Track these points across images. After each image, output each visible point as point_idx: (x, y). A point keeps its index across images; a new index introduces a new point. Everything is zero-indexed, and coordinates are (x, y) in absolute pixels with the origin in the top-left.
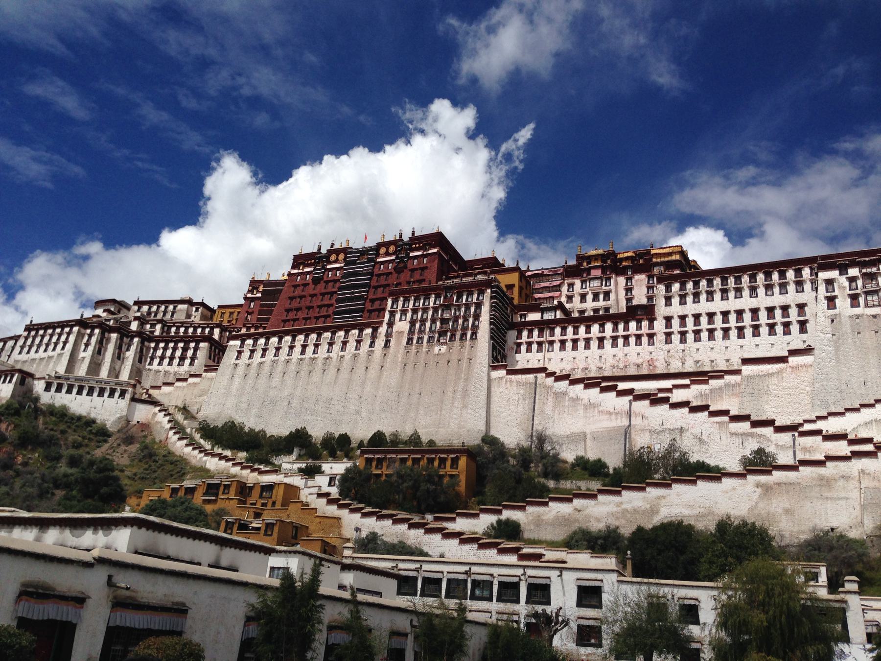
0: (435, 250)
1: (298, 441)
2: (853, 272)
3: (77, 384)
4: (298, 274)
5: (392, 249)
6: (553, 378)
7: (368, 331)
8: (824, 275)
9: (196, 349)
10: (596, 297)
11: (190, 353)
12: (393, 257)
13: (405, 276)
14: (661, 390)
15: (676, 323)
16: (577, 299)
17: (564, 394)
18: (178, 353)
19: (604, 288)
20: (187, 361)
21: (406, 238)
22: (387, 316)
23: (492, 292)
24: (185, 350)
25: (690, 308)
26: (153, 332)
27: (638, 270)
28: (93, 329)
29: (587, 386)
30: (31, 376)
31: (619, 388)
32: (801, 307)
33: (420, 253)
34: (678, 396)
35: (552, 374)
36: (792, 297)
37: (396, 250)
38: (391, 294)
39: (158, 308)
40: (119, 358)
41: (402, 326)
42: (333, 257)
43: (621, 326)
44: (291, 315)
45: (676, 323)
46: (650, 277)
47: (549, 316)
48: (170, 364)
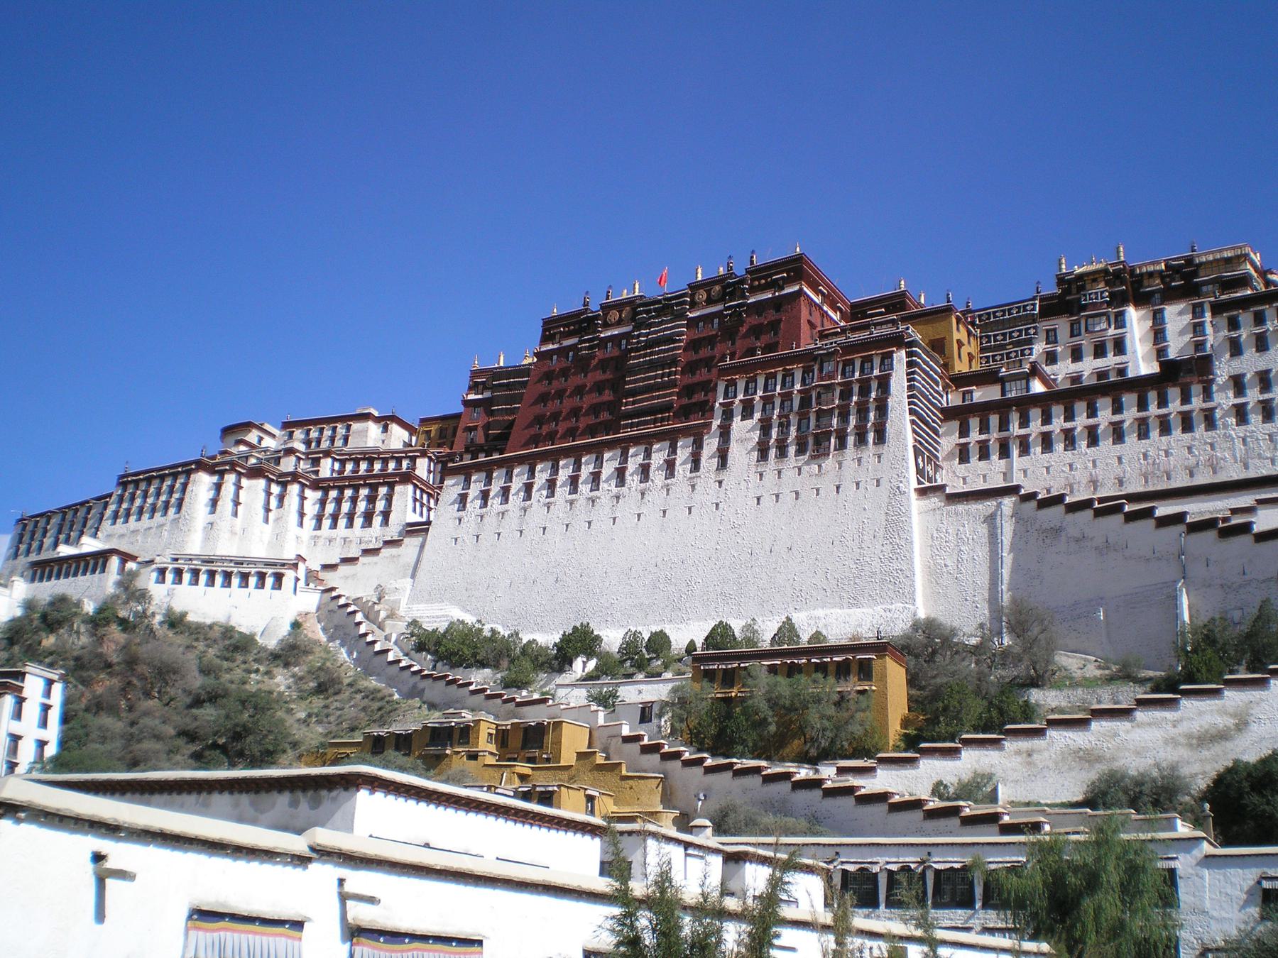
0: (796, 288)
3: (204, 568)
6: (1034, 504)
11: (380, 505)
14: (1235, 511)
17: (1057, 531)
18: (362, 506)
19: (1112, 331)
20: (377, 520)
21: (740, 271)
23: (909, 354)
24: (371, 499)
26: (317, 472)
27: (1170, 295)
28: (222, 474)
29: (1099, 513)
30: (134, 558)
31: (1158, 513)
35: (1032, 496)
37: (725, 294)
39: (321, 430)
40: (266, 520)
41: (744, 431)
48: (350, 524)
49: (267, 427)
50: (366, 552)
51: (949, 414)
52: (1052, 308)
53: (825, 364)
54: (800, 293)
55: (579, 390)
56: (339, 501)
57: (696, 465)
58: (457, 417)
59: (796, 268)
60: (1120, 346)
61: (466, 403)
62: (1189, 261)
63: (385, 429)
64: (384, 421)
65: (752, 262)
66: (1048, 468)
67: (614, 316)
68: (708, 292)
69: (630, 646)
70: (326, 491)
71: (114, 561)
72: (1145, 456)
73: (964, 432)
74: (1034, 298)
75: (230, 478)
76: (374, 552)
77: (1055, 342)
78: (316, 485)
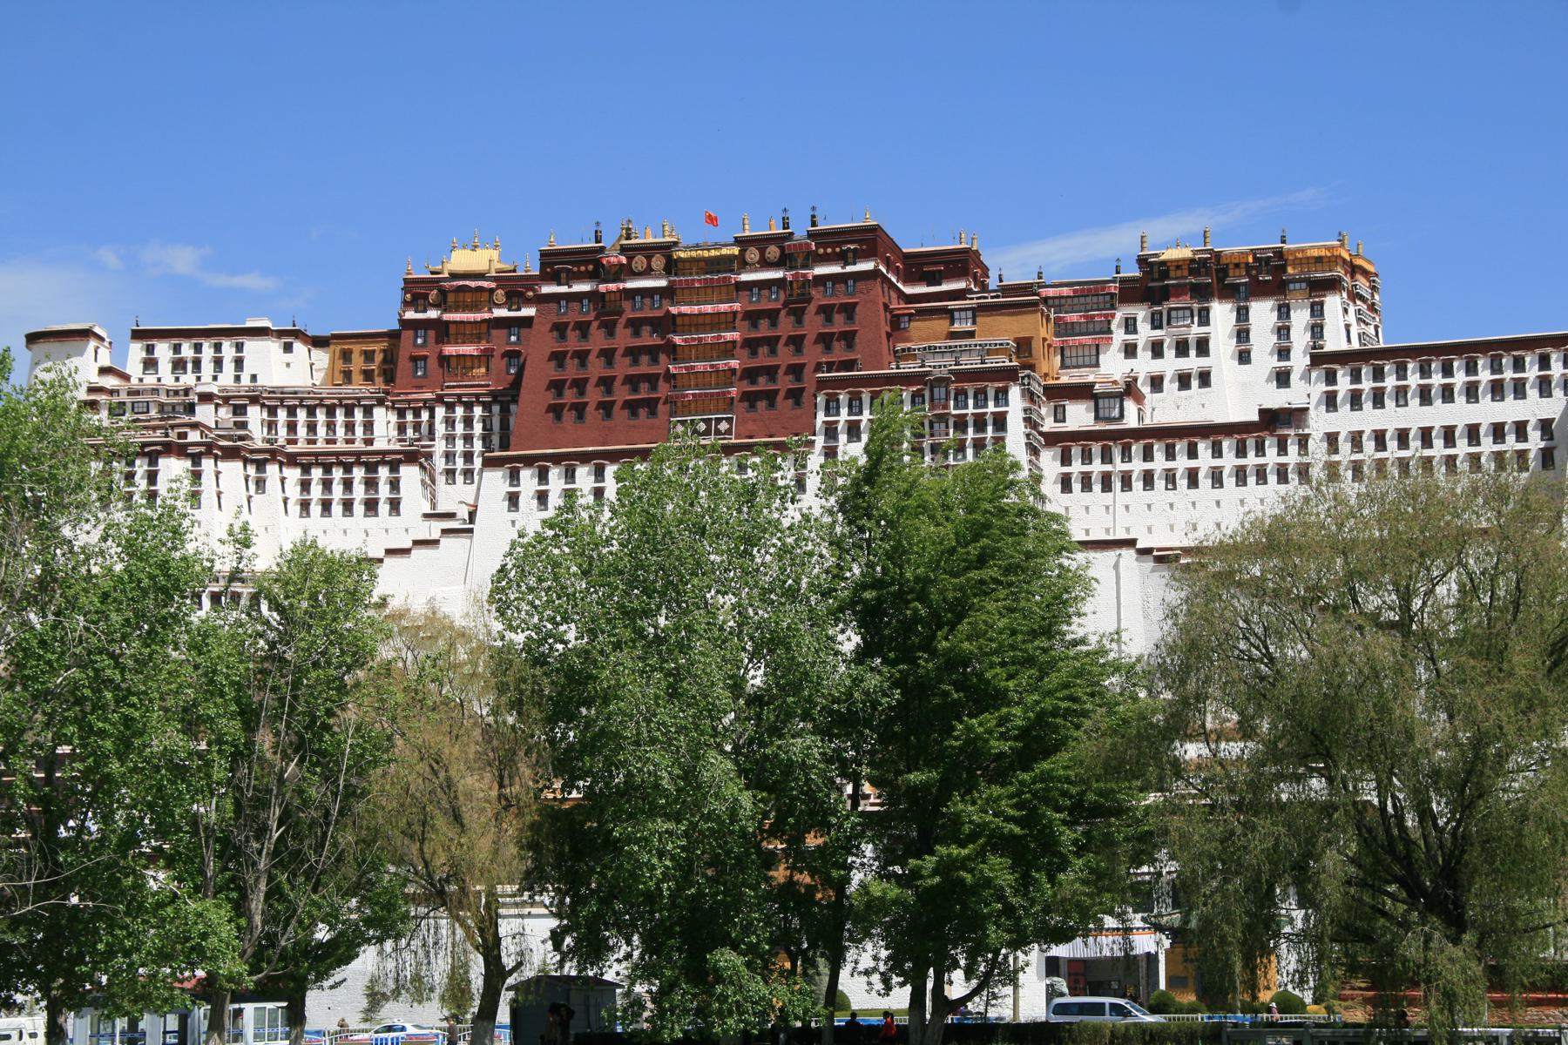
5: (773, 252)
11: (384, 491)
12: (777, 274)
13: (813, 325)
18: (359, 492)
19: (1196, 330)
20: (384, 508)
21: (800, 229)
24: (371, 484)
27: (1259, 290)
33: (835, 269)
35: (1146, 552)
38: (822, 385)
39: (198, 348)
43: (1251, 443)
44: (569, 396)
49: (97, 330)
50: (390, 552)
51: (1052, 439)
52: (1131, 292)
53: (936, 390)
54: (875, 274)
55: (608, 355)
56: (327, 485)
58: (393, 336)
59: (870, 240)
60: (1203, 347)
61: (406, 324)
62: (1279, 253)
63: (288, 348)
64: (289, 336)
65: (814, 224)
66: (1149, 506)
67: (640, 262)
68: (762, 252)
70: (306, 469)
72: (1242, 502)
74: (1113, 281)
75: (207, 464)
77: (1135, 331)
78: (292, 460)
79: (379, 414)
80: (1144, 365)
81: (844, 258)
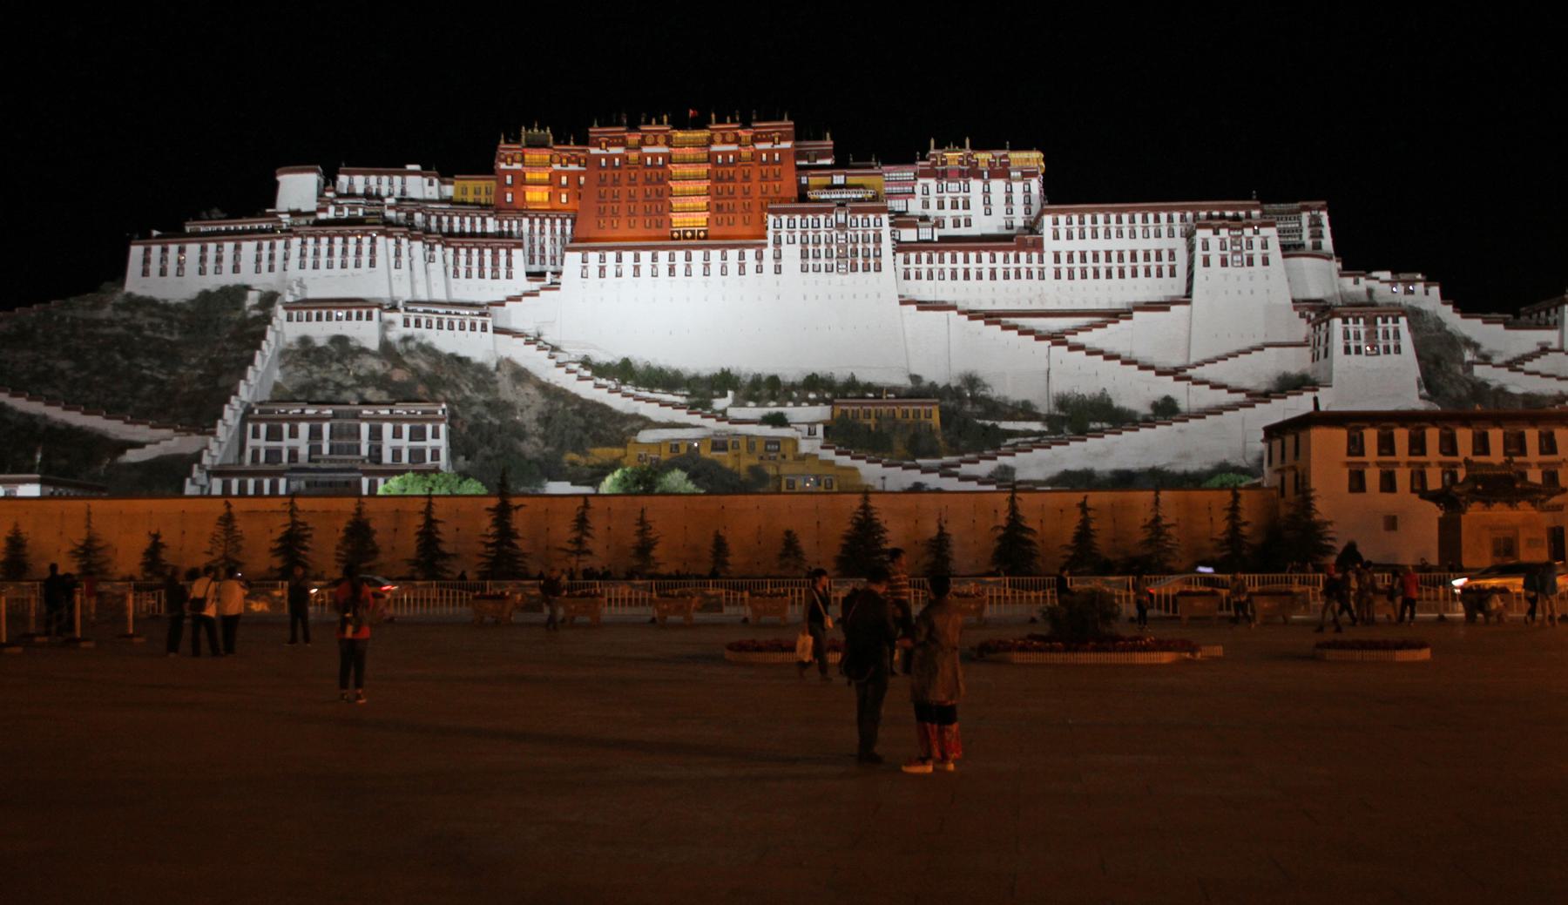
1: (724, 381)
2: (1224, 233)
4: (599, 156)
5: (730, 137)
7: (750, 254)
8: (1201, 234)
9: (509, 254)
10: (955, 206)
15: (1064, 257)
16: (933, 203)
22: (770, 234)
25: (1077, 245)
27: (994, 174)
32: (1172, 254)
33: (768, 146)
34: (1081, 338)
36: (1164, 243)
41: (791, 253)
42: (650, 138)
45: (1064, 257)
46: (1009, 183)
47: (925, 234)
48: (482, 276)
57: (759, 270)
60: (967, 206)
68: (724, 135)
69: (757, 382)
71: (376, 312)
73: (907, 261)
76: (517, 299)
79: (490, 221)
80: (933, 211)
81: (772, 140)
